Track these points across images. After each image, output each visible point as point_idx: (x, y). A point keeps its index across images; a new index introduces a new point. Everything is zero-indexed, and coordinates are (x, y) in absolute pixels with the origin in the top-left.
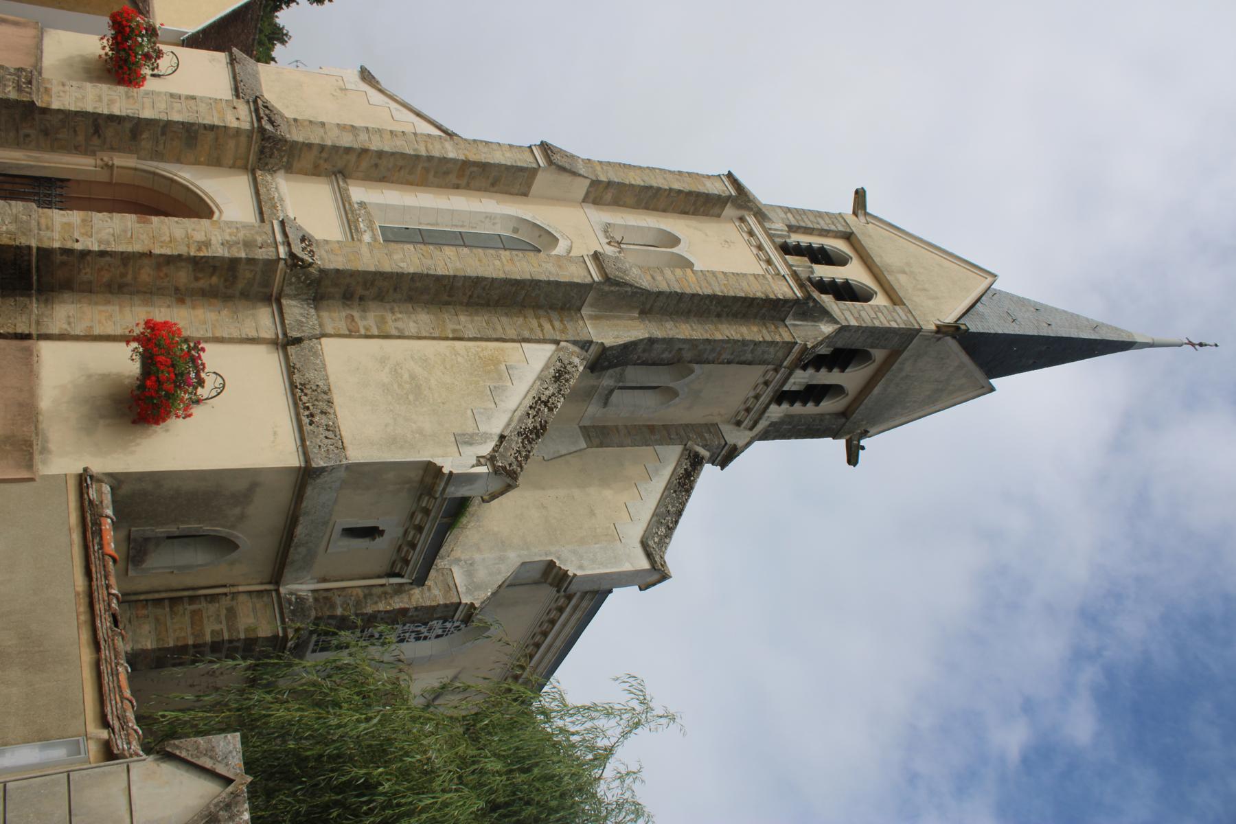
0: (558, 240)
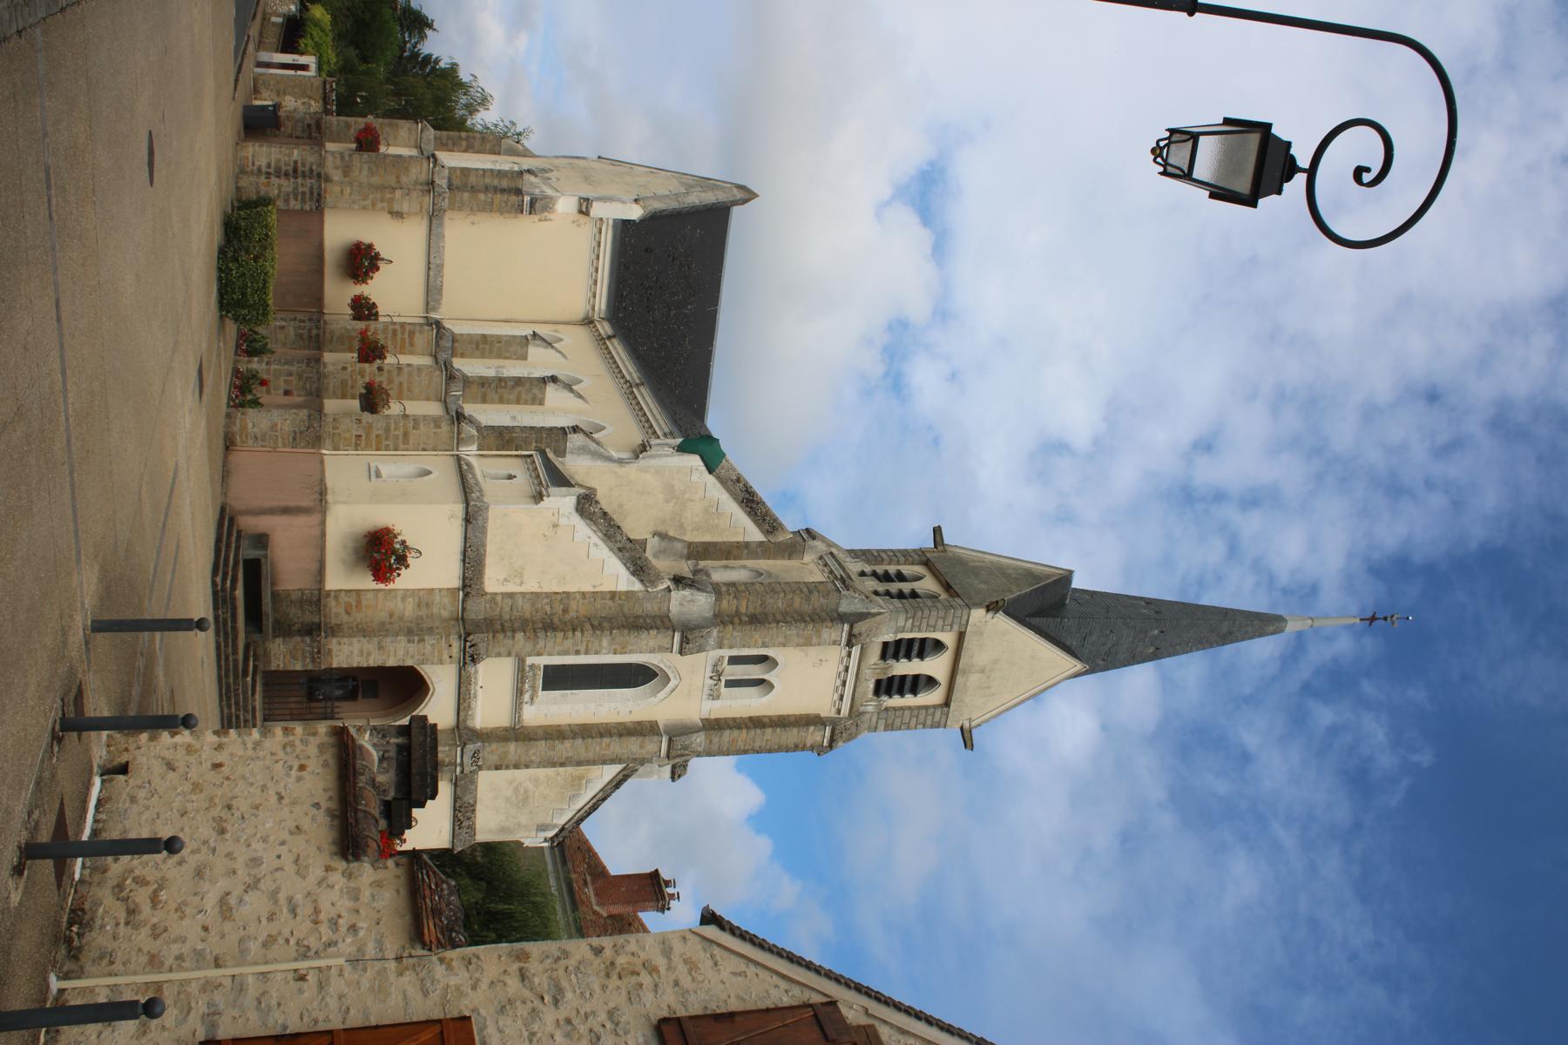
0: (670, 680)
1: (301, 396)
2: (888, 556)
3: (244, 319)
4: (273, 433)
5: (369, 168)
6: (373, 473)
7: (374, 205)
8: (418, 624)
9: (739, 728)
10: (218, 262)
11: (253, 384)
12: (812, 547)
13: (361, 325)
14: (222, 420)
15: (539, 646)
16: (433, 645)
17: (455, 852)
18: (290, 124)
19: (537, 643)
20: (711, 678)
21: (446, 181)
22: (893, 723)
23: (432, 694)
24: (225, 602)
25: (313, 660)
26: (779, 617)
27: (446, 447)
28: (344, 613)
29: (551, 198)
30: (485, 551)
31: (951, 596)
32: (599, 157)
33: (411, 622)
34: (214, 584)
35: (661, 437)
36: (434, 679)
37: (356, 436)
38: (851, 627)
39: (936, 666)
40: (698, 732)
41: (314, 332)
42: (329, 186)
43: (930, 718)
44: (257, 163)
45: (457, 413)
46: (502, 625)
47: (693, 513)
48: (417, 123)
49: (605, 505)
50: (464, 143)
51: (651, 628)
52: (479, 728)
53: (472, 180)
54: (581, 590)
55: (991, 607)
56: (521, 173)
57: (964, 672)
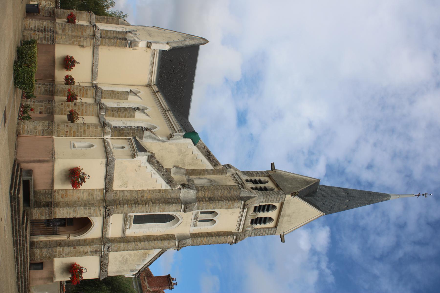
1: (46, 114)
2: (256, 174)
3: (24, 88)
4: (35, 130)
5: (72, 30)
6: (72, 146)
7: (73, 43)
8: (88, 202)
9: (204, 237)
10: (14, 67)
11: (28, 110)
12: (230, 171)
13: (68, 87)
14: (16, 126)
15: (133, 210)
16: (94, 210)
17: (101, 280)
18: (43, 12)
19: (132, 209)
20: (194, 219)
21: (100, 35)
22: (257, 233)
23: (93, 226)
24: (15, 199)
25: (49, 216)
26: (219, 198)
27: (99, 135)
28: (61, 198)
29: (137, 42)
30: (114, 176)
31: (279, 190)
32: (153, 26)
33: (86, 201)
34: (10, 193)
35: (177, 132)
36: (94, 221)
37: (66, 131)
38: (245, 202)
39: (273, 214)
40: (189, 238)
41: (51, 89)
42: (57, 36)
43: (270, 232)
44: (31, 26)
45: (103, 123)
46: (119, 202)
47: (188, 159)
48: (89, 13)
49: (158, 159)
50: (106, 20)
51: (174, 203)
52: (110, 237)
53: (109, 34)
54: (149, 189)
55: (293, 194)
56: (127, 32)
57: (283, 216)
